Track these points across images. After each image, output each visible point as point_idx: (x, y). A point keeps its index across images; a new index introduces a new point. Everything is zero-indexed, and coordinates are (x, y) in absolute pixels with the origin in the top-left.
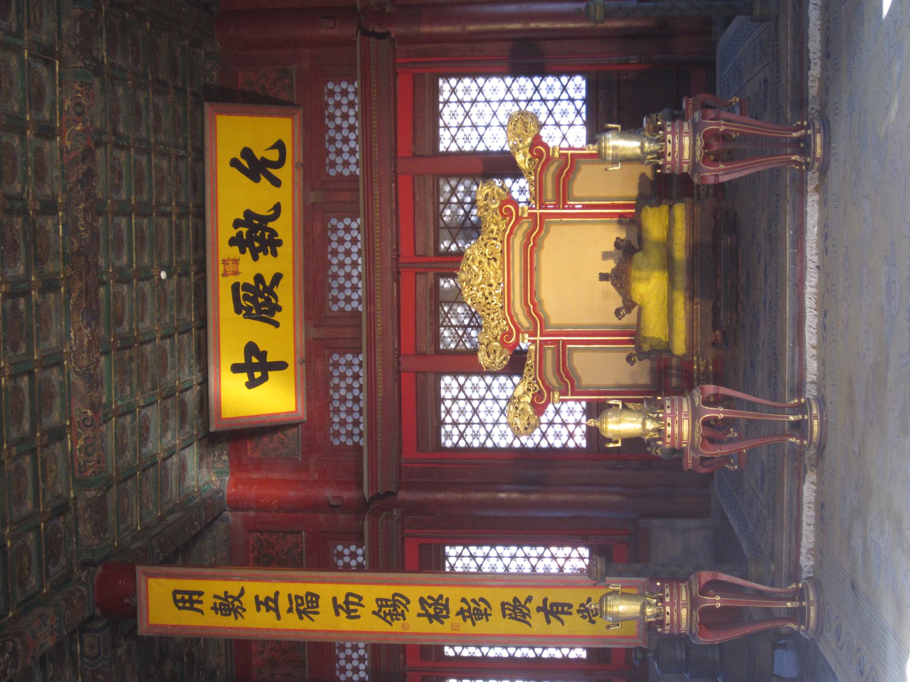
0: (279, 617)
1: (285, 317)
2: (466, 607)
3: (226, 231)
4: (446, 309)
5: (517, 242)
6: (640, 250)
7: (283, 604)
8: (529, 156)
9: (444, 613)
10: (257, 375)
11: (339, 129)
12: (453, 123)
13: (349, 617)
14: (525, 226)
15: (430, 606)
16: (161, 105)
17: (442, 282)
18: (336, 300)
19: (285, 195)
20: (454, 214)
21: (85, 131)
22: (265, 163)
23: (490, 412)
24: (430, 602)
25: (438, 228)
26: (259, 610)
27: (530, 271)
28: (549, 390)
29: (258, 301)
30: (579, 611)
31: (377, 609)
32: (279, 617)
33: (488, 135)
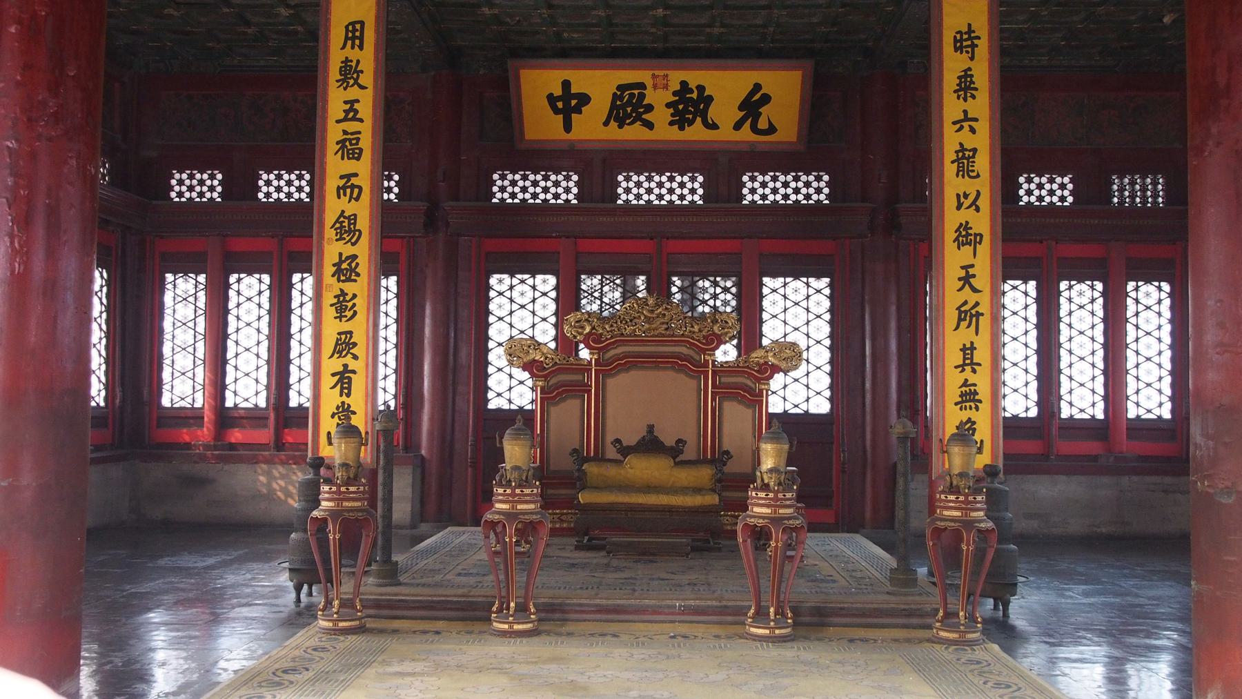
0: (338, 122)
1: (614, 133)
2: (348, 298)
3: (694, 78)
4: (618, 281)
5: (683, 350)
6: (676, 464)
7: (352, 126)
8: (762, 361)
9: (343, 278)
10: (560, 105)
11: (786, 185)
12: (789, 291)
13: (339, 188)
14: (697, 357)
15: (350, 265)
17: (643, 278)
18: (628, 179)
19: (726, 133)
20: (705, 290)
23: (522, 320)
24: (353, 265)
25: (692, 275)
26: (346, 102)
28: (545, 377)
29: (628, 107)
30: (343, 403)
31: (346, 214)
32: (338, 122)
33: (777, 323)
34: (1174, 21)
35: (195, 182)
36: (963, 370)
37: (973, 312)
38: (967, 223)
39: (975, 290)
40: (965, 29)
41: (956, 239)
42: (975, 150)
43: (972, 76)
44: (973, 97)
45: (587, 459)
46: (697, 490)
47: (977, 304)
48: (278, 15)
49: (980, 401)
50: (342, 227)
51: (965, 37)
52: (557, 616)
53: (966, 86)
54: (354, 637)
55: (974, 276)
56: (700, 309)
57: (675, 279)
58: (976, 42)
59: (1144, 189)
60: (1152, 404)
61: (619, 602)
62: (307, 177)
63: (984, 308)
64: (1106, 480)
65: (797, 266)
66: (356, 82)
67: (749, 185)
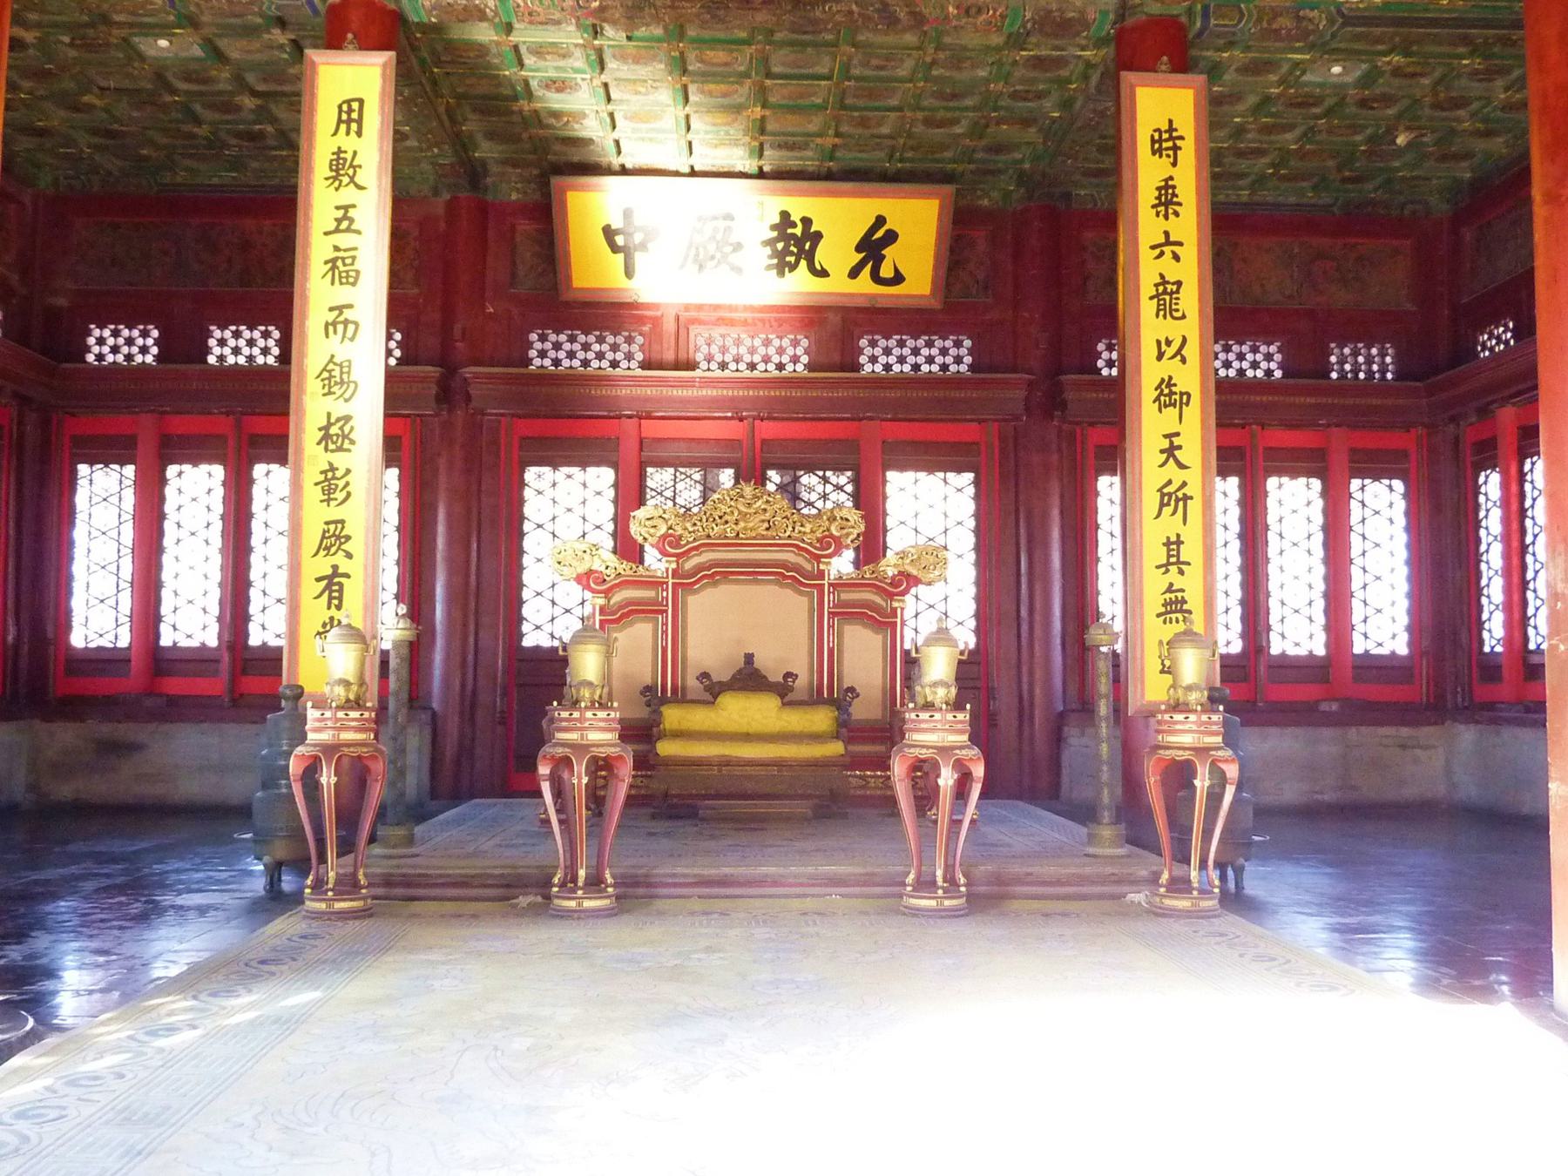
0: (326, 234)
5: (789, 557)
6: (784, 704)
7: (343, 240)
9: (332, 447)
13: (327, 325)
14: (808, 567)
15: (341, 428)
16: (958, 130)
20: (811, 489)
21: (947, 18)
22: (878, 260)
26: (338, 208)
27: (753, 572)
28: (607, 593)
32: (326, 234)
34: (1409, 145)
35: (121, 341)
36: (1167, 571)
37: (1180, 494)
38: (1170, 378)
39: (1181, 466)
40: (1165, 127)
41: (1157, 399)
42: (1179, 284)
43: (1174, 187)
44: (1176, 214)
45: (664, 701)
46: (816, 738)
47: (1184, 484)
48: (238, 108)
49: (1190, 612)
50: (329, 379)
51: (1165, 136)
52: (641, 891)
53: (1167, 199)
54: (357, 923)
55: (1180, 447)
56: (805, 511)
57: (772, 474)
58: (1179, 143)
59: (1369, 361)
60: (1383, 636)
61: (727, 870)
62: (276, 334)
63: (1194, 489)
64: (1327, 732)
65: (935, 456)
66: (352, 179)
67: (868, 351)
